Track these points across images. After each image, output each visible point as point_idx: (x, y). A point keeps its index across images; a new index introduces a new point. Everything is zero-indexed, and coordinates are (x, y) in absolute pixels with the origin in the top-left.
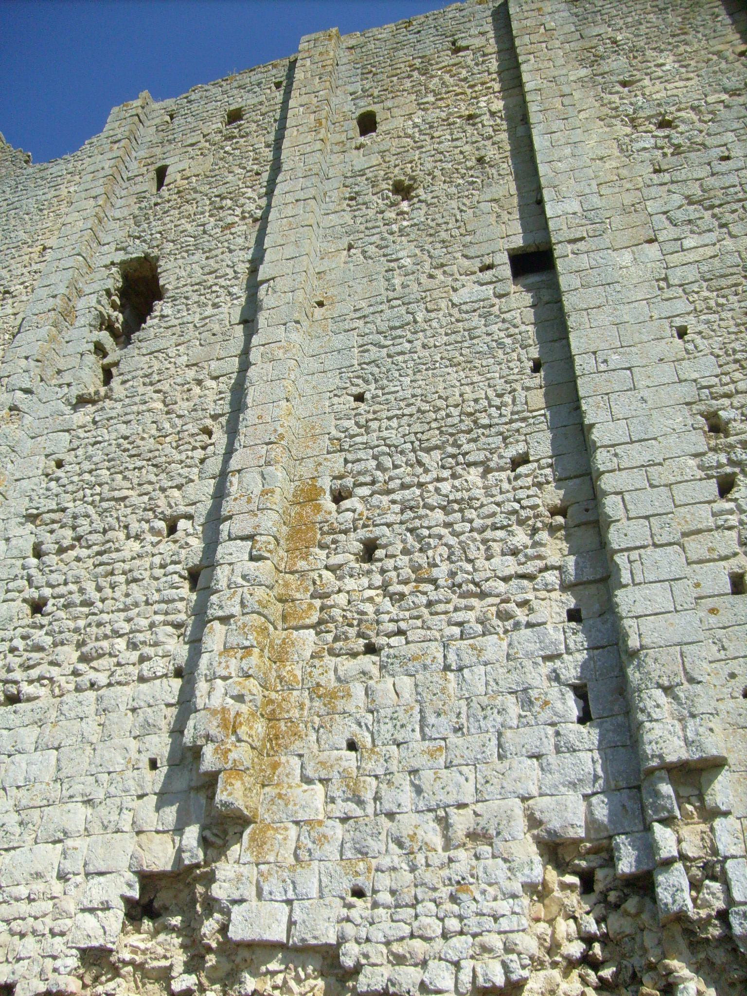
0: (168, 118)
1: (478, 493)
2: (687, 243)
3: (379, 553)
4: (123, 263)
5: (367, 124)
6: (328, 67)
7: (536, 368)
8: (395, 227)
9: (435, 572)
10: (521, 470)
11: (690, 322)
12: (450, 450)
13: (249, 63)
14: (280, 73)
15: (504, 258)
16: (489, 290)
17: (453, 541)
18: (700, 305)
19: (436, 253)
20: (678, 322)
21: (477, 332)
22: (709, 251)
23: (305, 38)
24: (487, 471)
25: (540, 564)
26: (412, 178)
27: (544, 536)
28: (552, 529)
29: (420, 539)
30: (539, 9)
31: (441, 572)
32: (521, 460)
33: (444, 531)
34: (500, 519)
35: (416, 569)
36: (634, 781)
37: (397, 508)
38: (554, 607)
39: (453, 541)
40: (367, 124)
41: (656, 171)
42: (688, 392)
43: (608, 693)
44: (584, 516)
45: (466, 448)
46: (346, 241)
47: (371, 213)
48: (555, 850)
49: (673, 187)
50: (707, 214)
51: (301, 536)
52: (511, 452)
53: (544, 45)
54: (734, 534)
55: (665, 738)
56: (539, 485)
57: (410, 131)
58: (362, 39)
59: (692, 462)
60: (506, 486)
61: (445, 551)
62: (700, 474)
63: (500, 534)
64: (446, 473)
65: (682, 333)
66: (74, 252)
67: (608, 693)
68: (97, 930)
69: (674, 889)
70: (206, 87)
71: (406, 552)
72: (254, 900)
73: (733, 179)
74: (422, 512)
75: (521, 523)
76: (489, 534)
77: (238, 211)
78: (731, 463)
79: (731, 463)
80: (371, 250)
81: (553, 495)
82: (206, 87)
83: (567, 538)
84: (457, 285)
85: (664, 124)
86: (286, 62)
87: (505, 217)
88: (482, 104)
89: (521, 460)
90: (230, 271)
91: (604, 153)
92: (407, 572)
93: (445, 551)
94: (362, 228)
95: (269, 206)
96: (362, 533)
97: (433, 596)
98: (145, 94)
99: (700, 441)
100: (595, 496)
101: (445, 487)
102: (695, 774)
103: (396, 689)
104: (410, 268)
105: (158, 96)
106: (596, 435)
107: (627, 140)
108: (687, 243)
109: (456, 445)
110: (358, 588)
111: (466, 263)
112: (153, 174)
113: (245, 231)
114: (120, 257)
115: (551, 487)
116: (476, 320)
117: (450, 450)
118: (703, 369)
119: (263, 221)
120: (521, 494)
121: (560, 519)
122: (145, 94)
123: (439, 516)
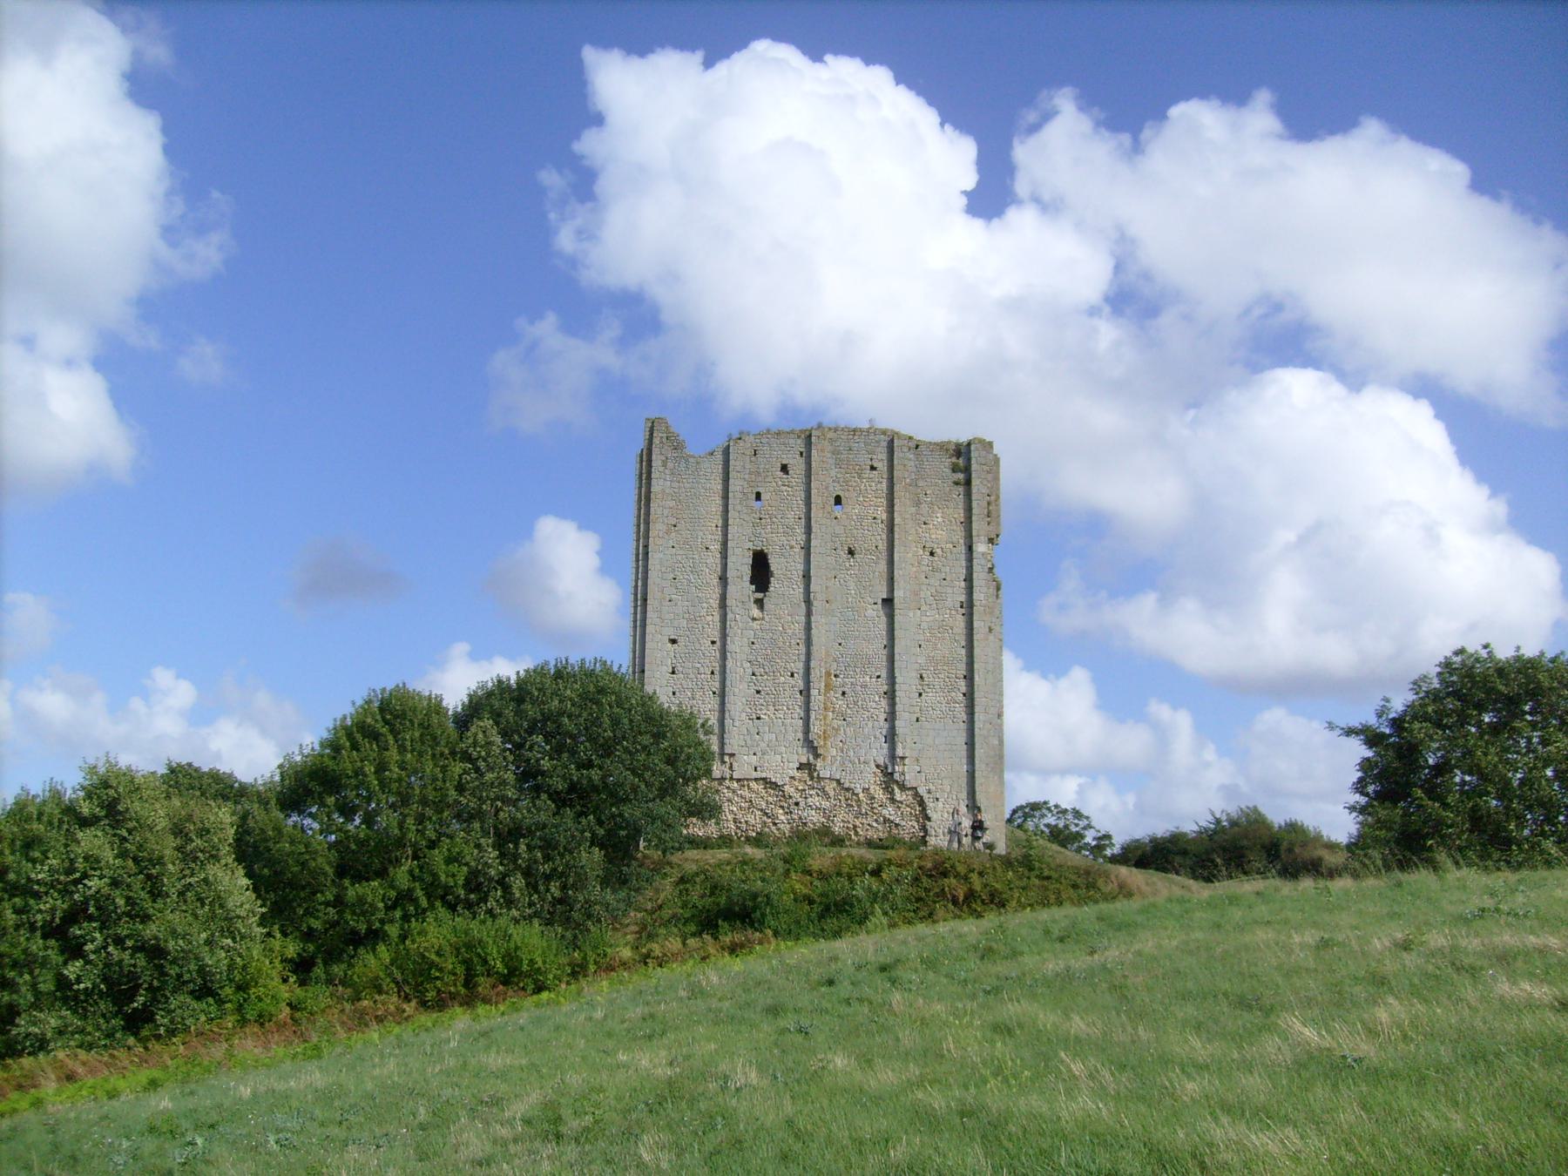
36: (893, 756)
38: (883, 716)
43: (891, 737)
44: (891, 695)
48: (878, 766)
51: (828, 687)
55: (899, 752)
67: (891, 737)
68: (791, 773)
69: (897, 776)
72: (824, 769)
81: (885, 688)
99: (917, 681)
102: (903, 758)
103: (850, 731)
110: (840, 704)
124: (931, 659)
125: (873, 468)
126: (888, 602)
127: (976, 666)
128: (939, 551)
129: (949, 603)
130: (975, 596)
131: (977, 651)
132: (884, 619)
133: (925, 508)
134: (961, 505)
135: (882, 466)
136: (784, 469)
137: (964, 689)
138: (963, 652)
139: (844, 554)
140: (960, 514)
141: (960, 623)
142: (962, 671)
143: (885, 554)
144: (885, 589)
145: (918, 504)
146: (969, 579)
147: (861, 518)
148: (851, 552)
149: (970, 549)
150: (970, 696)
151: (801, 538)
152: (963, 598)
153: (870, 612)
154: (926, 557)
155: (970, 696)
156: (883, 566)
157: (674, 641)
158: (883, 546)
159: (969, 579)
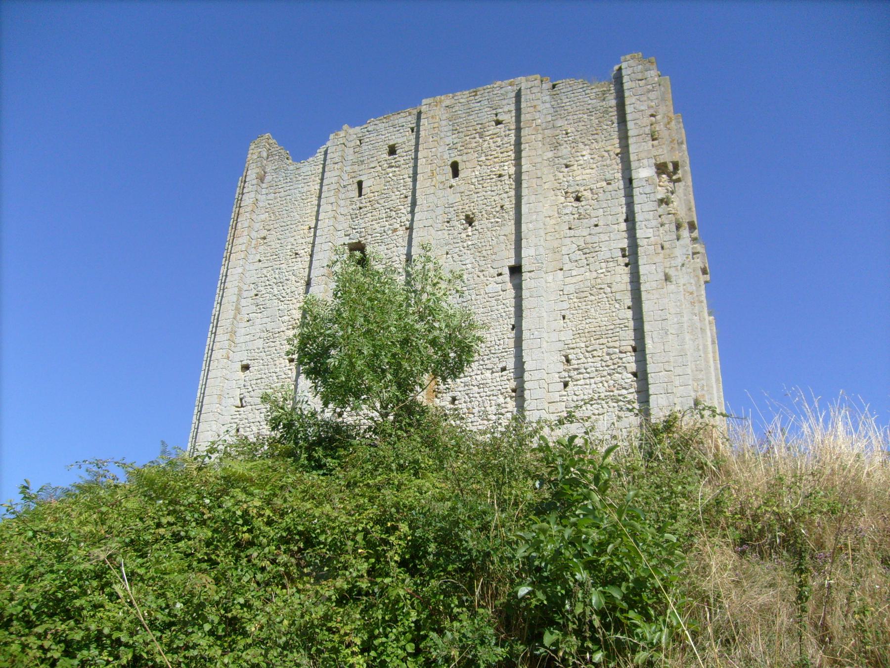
0: (358, 143)
1: (489, 381)
2: (574, 273)
3: (456, 402)
4: (349, 244)
5: (455, 169)
6: (436, 111)
7: (513, 329)
8: (465, 245)
9: (474, 411)
10: (504, 373)
11: (567, 313)
12: (481, 362)
13: (397, 109)
14: (412, 119)
15: (506, 271)
16: (499, 287)
17: (480, 399)
18: (572, 306)
19: (481, 263)
20: (563, 313)
21: (494, 308)
22: (579, 278)
23: (424, 101)
24: (493, 372)
25: (506, 410)
26: (473, 214)
27: (508, 399)
28: (511, 397)
29: (470, 398)
30: (535, 107)
31: (475, 411)
32: (504, 369)
33: (478, 395)
34: (495, 392)
35: (468, 409)
37: (463, 385)
39: (480, 399)
40: (455, 169)
41: (570, 229)
42: (561, 346)
45: (486, 362)
46: (446, 248)
47: (456, 232)
49: (573, 239)
50: (583, 257)
52: (501, 366)
53: (533, 137)
54: (564, 404)
56: (508, 380)
57: (473, 181)
58: (453, 101)
59: (557, 375)
60: (498, 379)
61: (477, 403)
62: (559, 380)
63: (495, 398)
64: (479, 372)
65: (564, 317)
66: (327, 240)
70: (377, 122)
71: (465, 402)
73: (595, 239)
74: (471, 387)
75: (502, 394)
76: (491, 398)
77: (399, 220)
78: (570, 377)
79: (570, 377)
80: (455, 256)
81: (513, 384)
82: (377, 122)
83: (516, 401)
84: (488, 282)
85: (578, 199)
86: (415, 112)
87: (509, 246)
88: (506, 168)
89: (504, 369)
90: (397, 259)
91: (551, 214)
92: (465, 410)
93: (477, 403)
94: (452, 242)
95: (412, 220)
96: (451, 394)
97: (473, 419)
98: (345, 127)
99: (561, 367)
100: (523, 390)
101: (479, 377)
104: (471, 270)
105: (352, 126)
106: (525, 366)
107: (561, 206)
108: (574, 273)
109: (483, 360)
111: (492, 270)
112: (356, 186)
113: (401, 232)
114: (347, 240)
115: (512, 381)
116: (494, 303)
117: (481, 362)
118: (567, 336)
119: (410, 229)
120: (503, 383)
121: (514, 394)
122: (345, 127)
123: (476, 389)
124: (578, 334)
125: (498, 123)
126: (516, 270)
127: (647, 327)
128: (587, 194)
129: (604, 254)
130: (639, 234)
131: (646, 306)
132: (511, 293)
133: (565, 150)
134: (615, 135)
135: (509, 118)
136: (392, 151)
137: (633, 367)
138: (629, 314)
139: (459, 224)
140: (615, 146)
141: (623, 276)
142: (628, 338)
143: (512, 213)
144: (512, 253)
145: (556, 146)
146: (630, 219)
147: (482, 179)
148: (470, 221)
149: (629, 182)
150: (641, 375)
151: (406, 218)
152: (625, 243)
153: (493, 287)
154: (571, 203)
155: (641, 375)
156: (511, 227)
157: (246, 368)
158: (510, 205)
159: (630, 219)
